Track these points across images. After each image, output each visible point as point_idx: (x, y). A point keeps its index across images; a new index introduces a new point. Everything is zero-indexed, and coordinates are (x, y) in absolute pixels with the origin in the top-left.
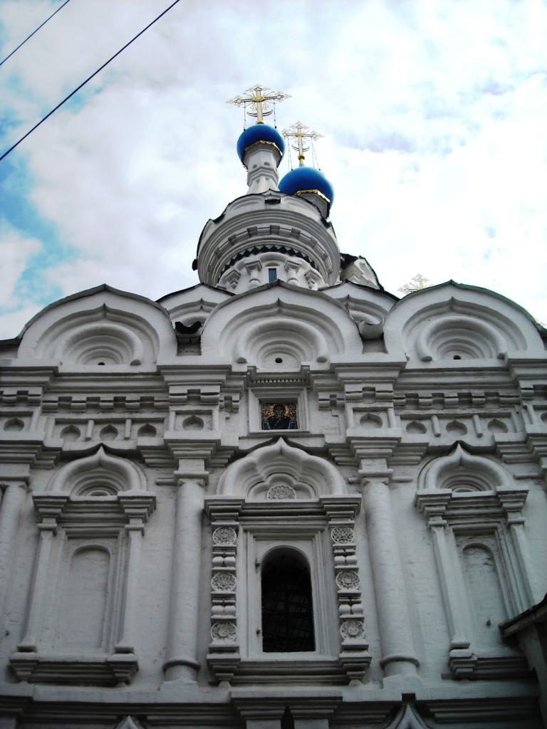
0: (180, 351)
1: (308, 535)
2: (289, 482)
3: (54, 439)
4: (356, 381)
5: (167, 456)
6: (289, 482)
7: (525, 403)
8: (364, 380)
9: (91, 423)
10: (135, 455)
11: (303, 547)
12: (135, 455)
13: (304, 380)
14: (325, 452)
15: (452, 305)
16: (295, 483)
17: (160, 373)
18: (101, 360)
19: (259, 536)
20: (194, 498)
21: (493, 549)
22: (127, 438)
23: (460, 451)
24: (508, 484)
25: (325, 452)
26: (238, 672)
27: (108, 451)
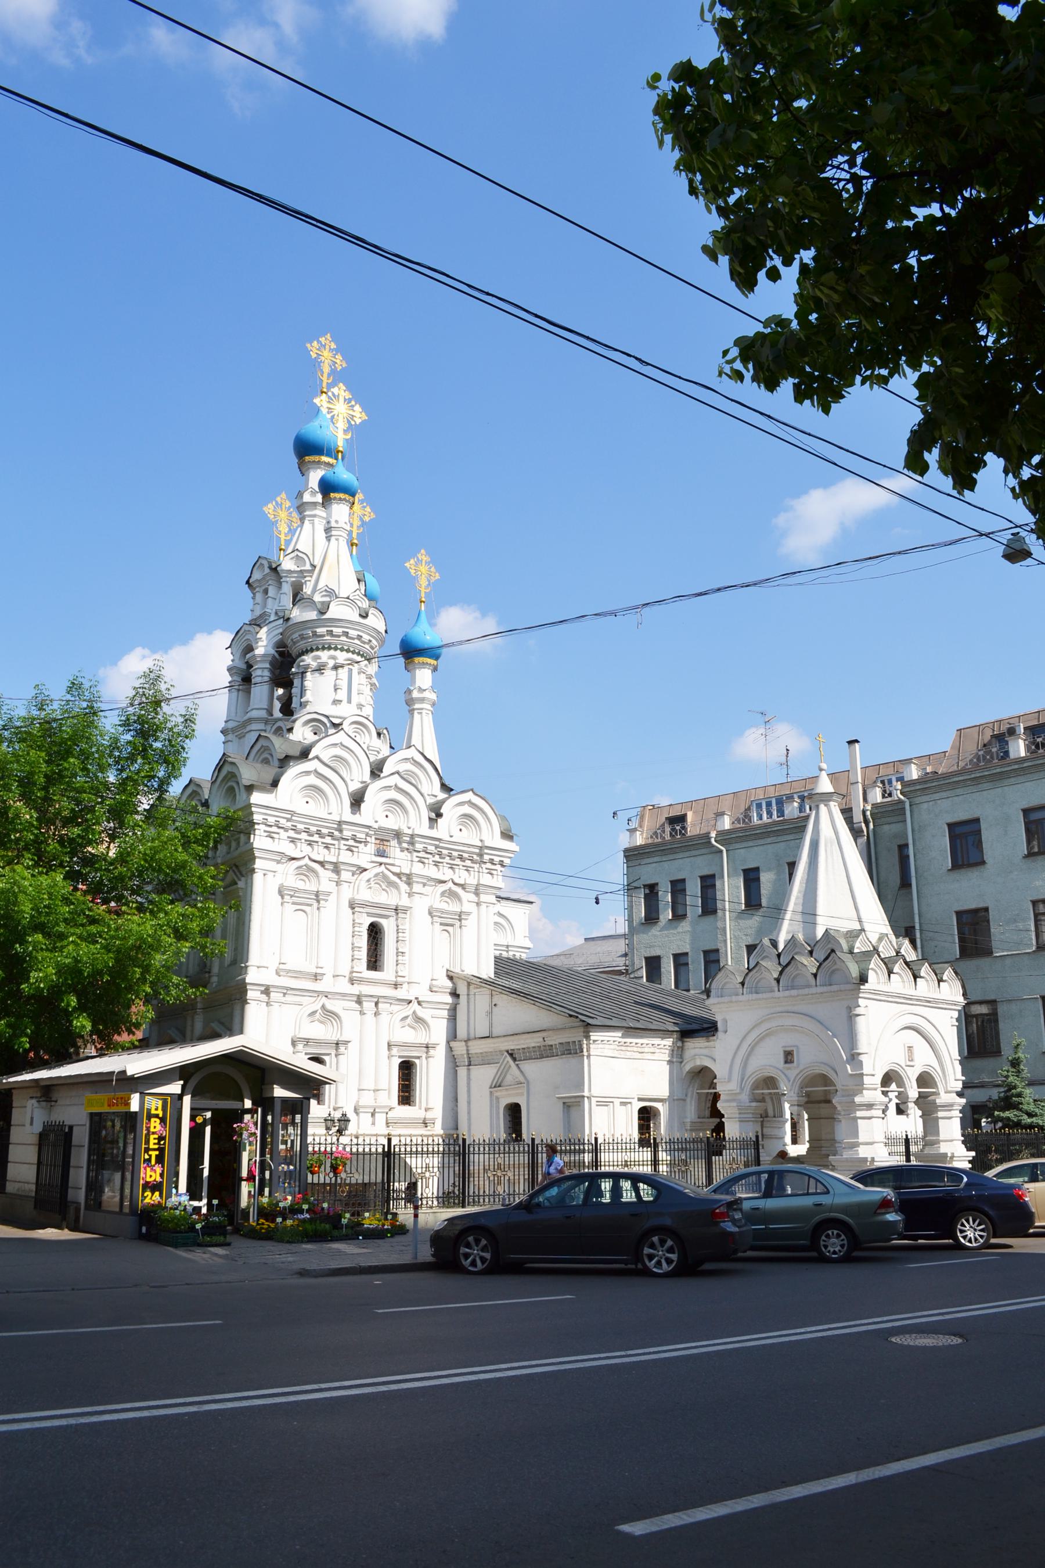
0: (353, 813)
1: (386, 917)
2: (381, 886)
3: (291, 850)
4: (421, 843)
5: (336, 868)
6: (381, 886)
7: (483, 865)
8: (425, 843)
9: (303, 841)
10: (322, 864)
11: (383, 922)
12: (322, 864)
13: (398, 835)
14: (398, 875)
15: (470, 803)
16: (384, 887)
17: (340, 823)
18: (308, 799)
19: (369, 914)
20: (347, 893)
21: (452, 933)
22: (320, 853)
23: (450, 885)
24: (467, 907)
25: (398, 875)
26: (361, 981)
27: (310, 859)
